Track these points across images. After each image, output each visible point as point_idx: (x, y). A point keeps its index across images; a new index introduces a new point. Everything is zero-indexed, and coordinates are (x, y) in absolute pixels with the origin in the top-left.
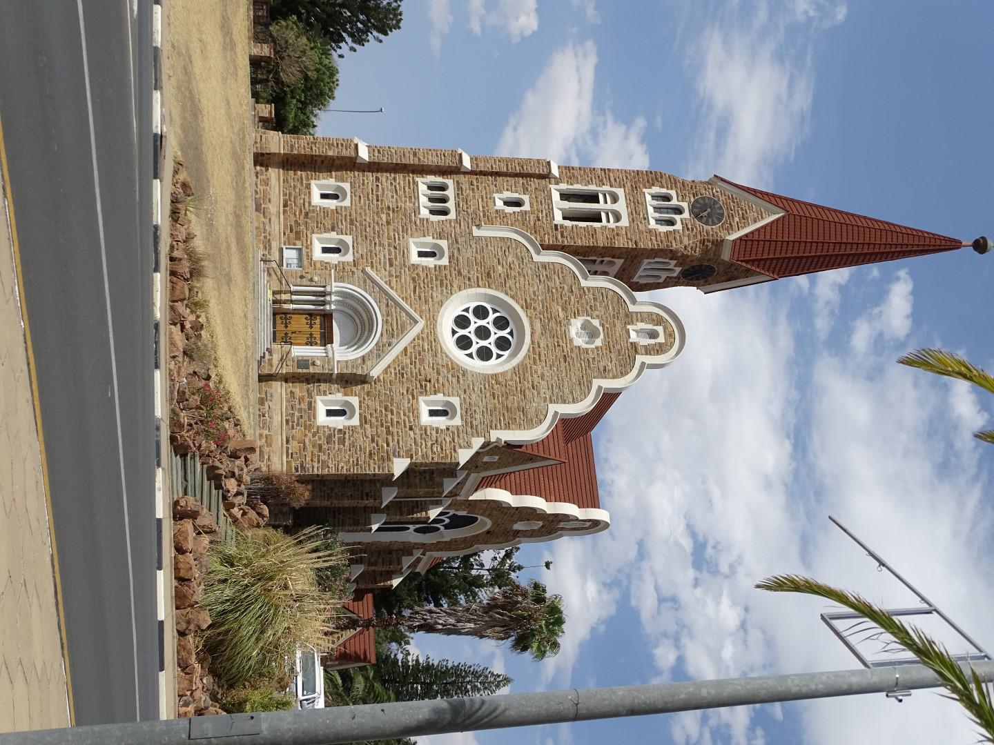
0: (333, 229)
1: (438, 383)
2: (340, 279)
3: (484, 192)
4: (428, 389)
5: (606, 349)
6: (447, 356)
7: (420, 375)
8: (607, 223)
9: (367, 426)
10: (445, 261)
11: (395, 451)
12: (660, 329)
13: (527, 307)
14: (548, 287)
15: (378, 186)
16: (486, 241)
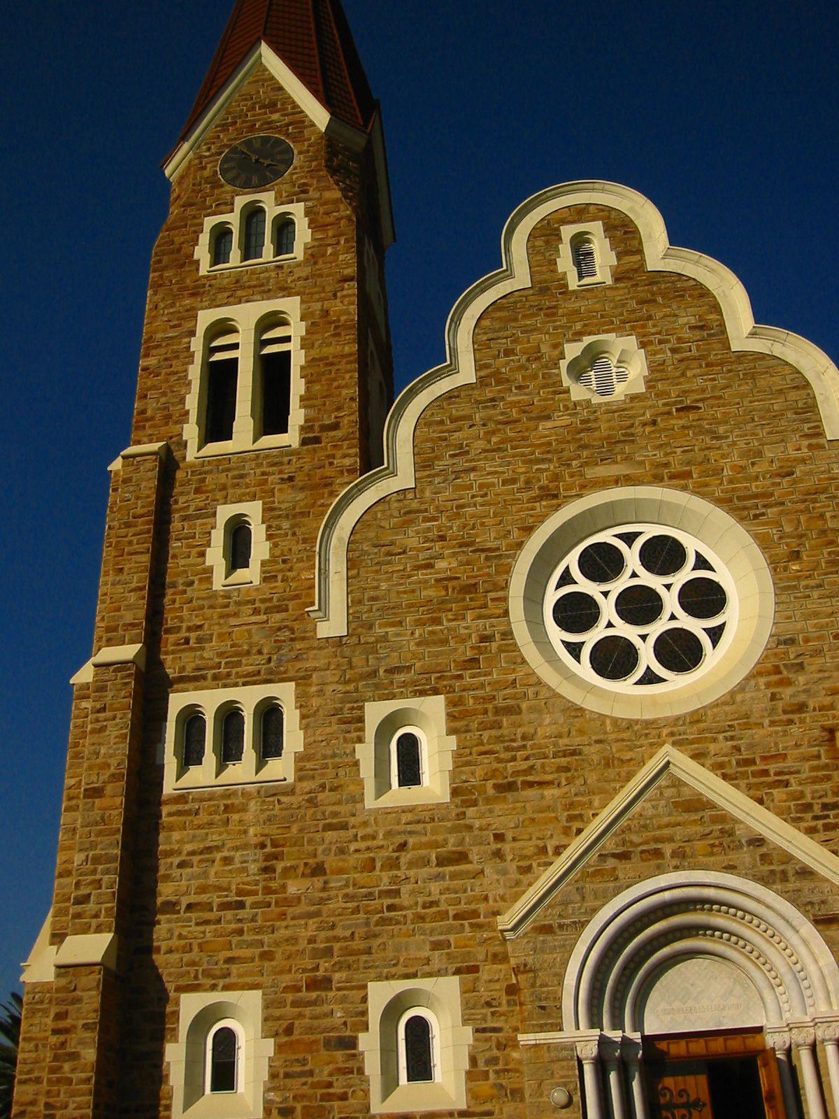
0: (351, 1043)
2: (549, 1016)
5: (643, 327)
6: (741, 688)
7: (818, 757)
10: (435, 707)
12: (568, 232)
13: (553, 497)
14: (485, 451)
15: (190, 907)
16: (360, 602)
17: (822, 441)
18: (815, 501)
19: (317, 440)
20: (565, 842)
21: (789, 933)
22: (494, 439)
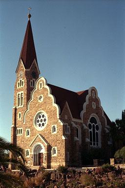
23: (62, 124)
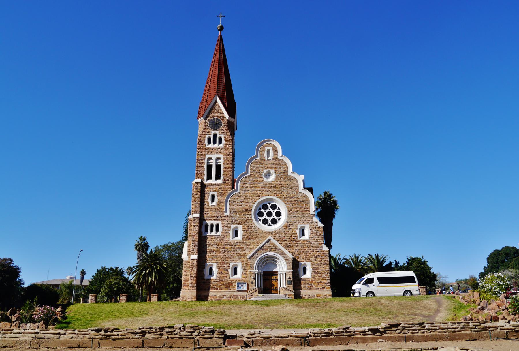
0: (228, 270)
1: (292, 232)
2: (252, 268)
3: (208, 209)
4: (295, 236)
5: (276, 169)
7: (289, 238)
8: (221, 163)
9: (311, 259)
11: (320, 249)
14: (250, 188)
16: (231, 210)
17: (298, 192)
18: (296, 202)
19: (225, 182)
20: (256, 247)
21: (282, 261)
22: (252, 186)
23: (321, 225)
